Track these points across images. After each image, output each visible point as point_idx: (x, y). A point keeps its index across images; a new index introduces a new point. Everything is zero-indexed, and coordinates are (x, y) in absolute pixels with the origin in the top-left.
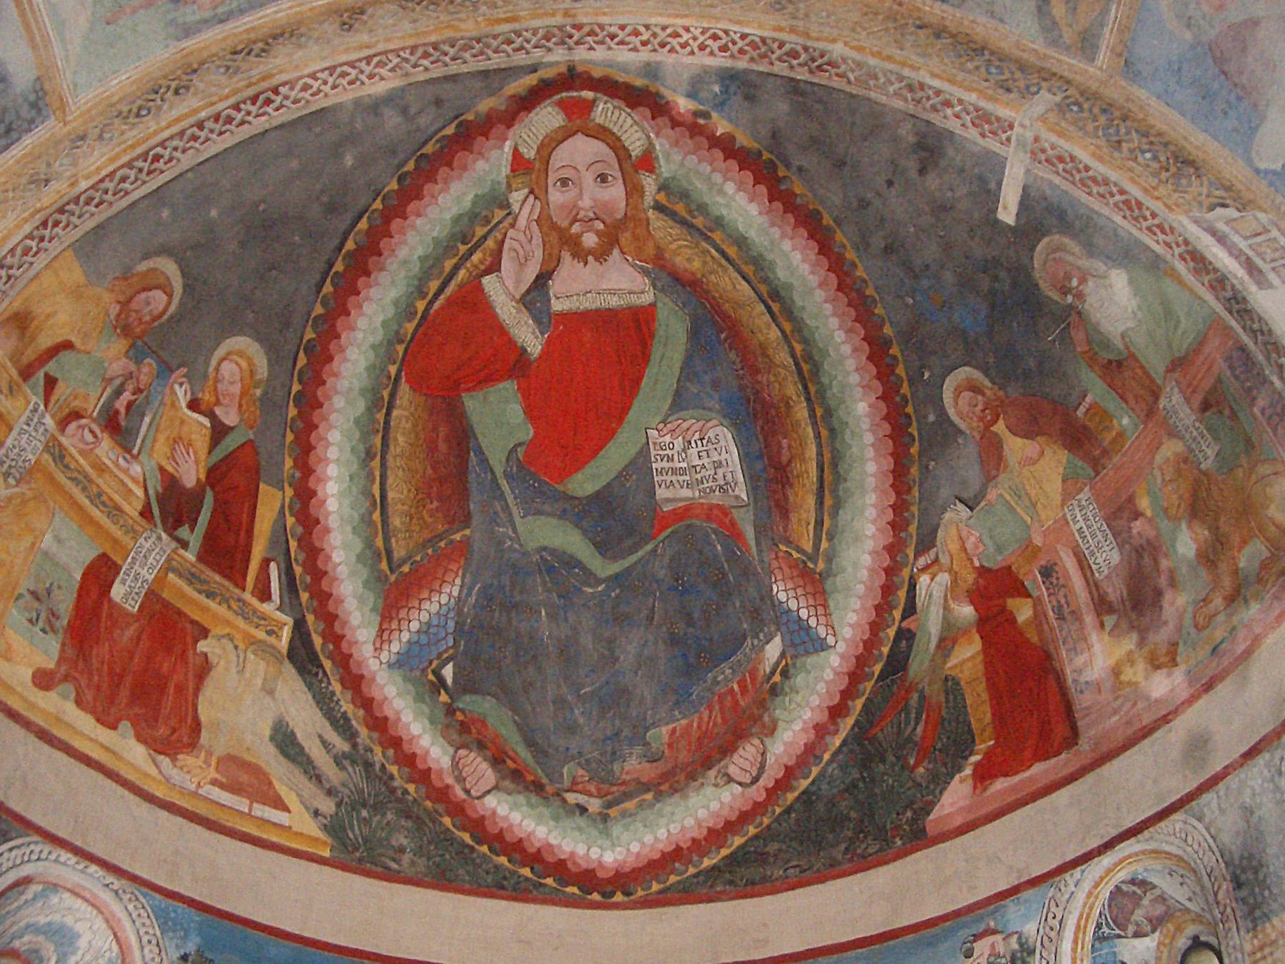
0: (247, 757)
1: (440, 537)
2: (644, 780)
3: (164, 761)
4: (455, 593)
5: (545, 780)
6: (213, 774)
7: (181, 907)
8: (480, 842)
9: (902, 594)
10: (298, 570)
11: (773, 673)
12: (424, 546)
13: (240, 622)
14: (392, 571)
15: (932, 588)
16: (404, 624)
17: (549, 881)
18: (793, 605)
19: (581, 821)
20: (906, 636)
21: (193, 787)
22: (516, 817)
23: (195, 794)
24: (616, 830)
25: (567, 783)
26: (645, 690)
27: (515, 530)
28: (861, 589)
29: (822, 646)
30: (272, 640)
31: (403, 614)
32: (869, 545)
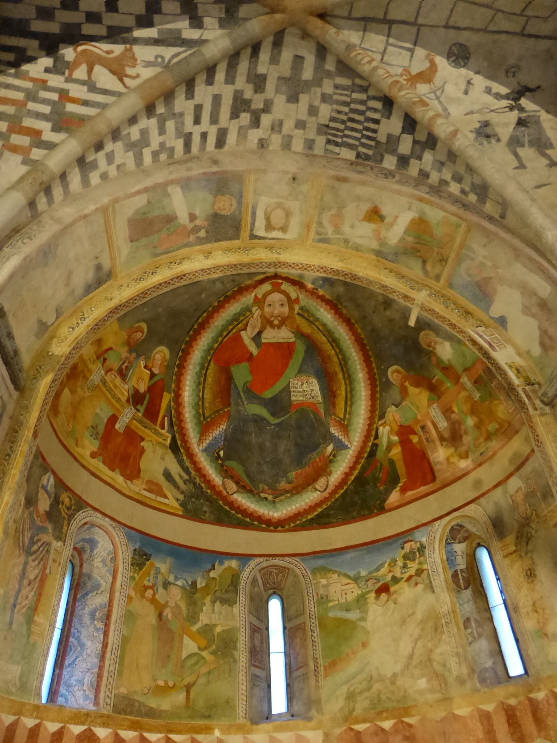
0: (155, 481)
1: (220, 410)
2: (287, 489)
3: (129, 482)
4: (225, 428)
5: (253, 489)
6: (144, 486)
7: (134, 532)
8: (232, 510)
9: (374, 432)
10: (174, 419)
11: (330, 455)
12: (216, 412)
13: (154, 436)
14: (204, 420)
15: (384, 431)
16: (208, 437)
17: (256, 523)
18: (337, 434)
19: (266, 503)
20: (375, 446)
21: (138, 491)
22: (244, 501)
23: (138, 493)
24: (278, 506)
25: (261, 490)
26: (287, 460)
27: (245, 408)
28: (359, 430)
29: (346, 448)
30: (164, 442)
31: (207, 434)
32: (363, 417)
